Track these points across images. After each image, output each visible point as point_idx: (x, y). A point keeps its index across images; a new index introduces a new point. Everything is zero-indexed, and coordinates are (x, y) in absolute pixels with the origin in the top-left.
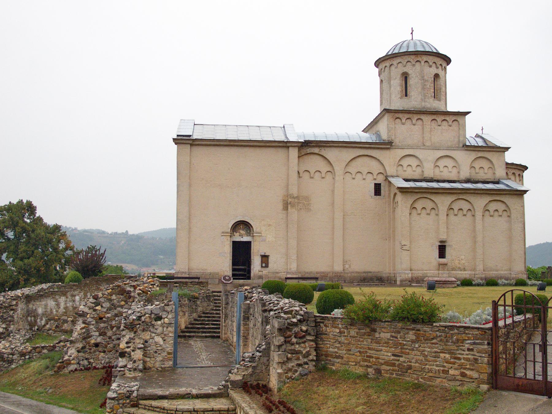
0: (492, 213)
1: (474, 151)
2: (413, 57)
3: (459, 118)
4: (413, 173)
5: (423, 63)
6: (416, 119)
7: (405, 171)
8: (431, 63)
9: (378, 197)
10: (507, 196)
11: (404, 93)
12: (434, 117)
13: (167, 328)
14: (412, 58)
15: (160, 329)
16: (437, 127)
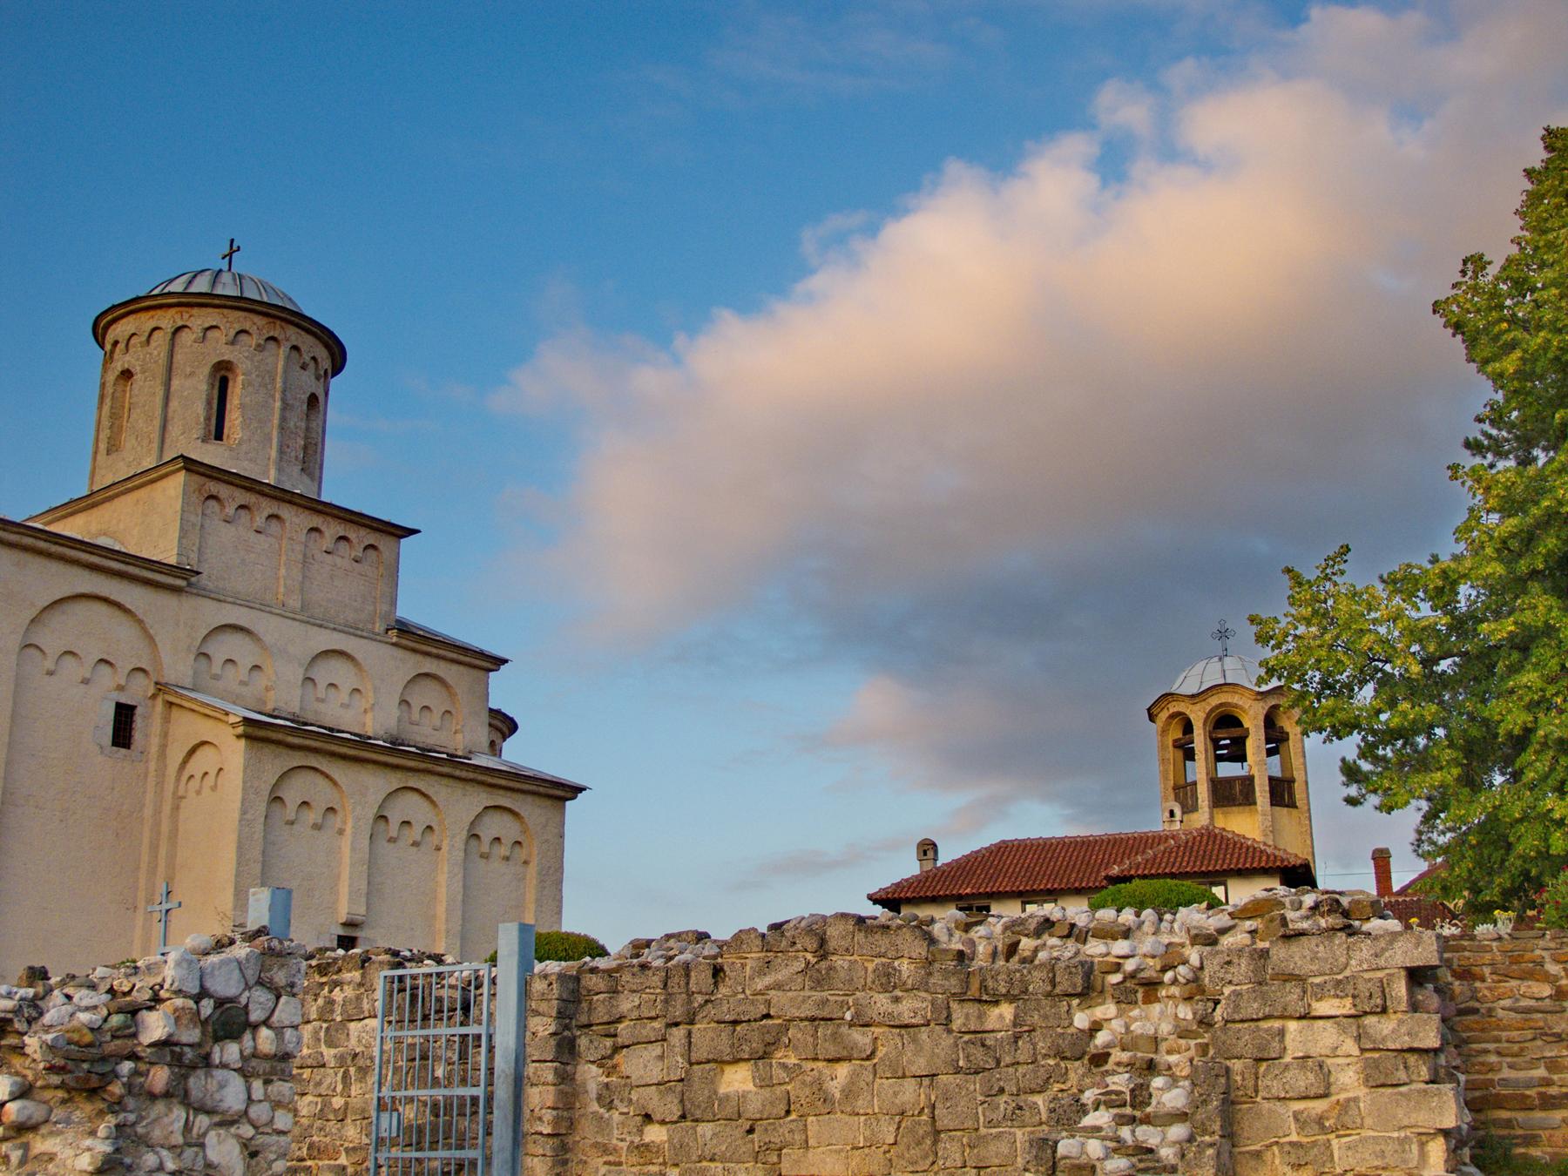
0: (485, 848)
1: (414, 651)
2: (260, 321)
3: (384, 542)
4: (244, 690)
5: (283, 351)
6: (266, 514)
7: (216, 677)
9: (123, 751)
10: (530, 798)
11: (213, 428)
12: (316, 521)
13: (267, 1082)
14: (254, 323)
15: (236, 1084)
16: (321, 556)
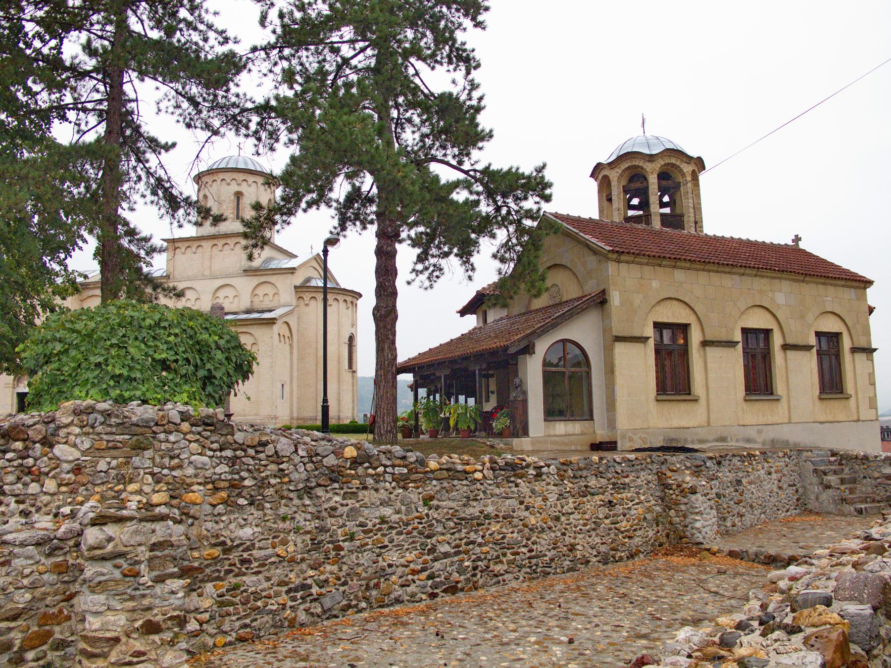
8: (228, 181)
12: (215, 242)
